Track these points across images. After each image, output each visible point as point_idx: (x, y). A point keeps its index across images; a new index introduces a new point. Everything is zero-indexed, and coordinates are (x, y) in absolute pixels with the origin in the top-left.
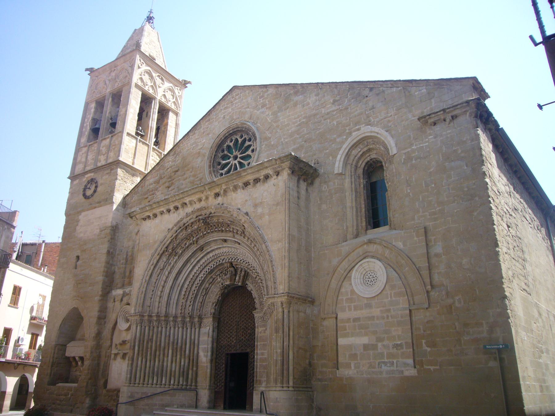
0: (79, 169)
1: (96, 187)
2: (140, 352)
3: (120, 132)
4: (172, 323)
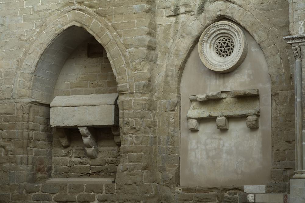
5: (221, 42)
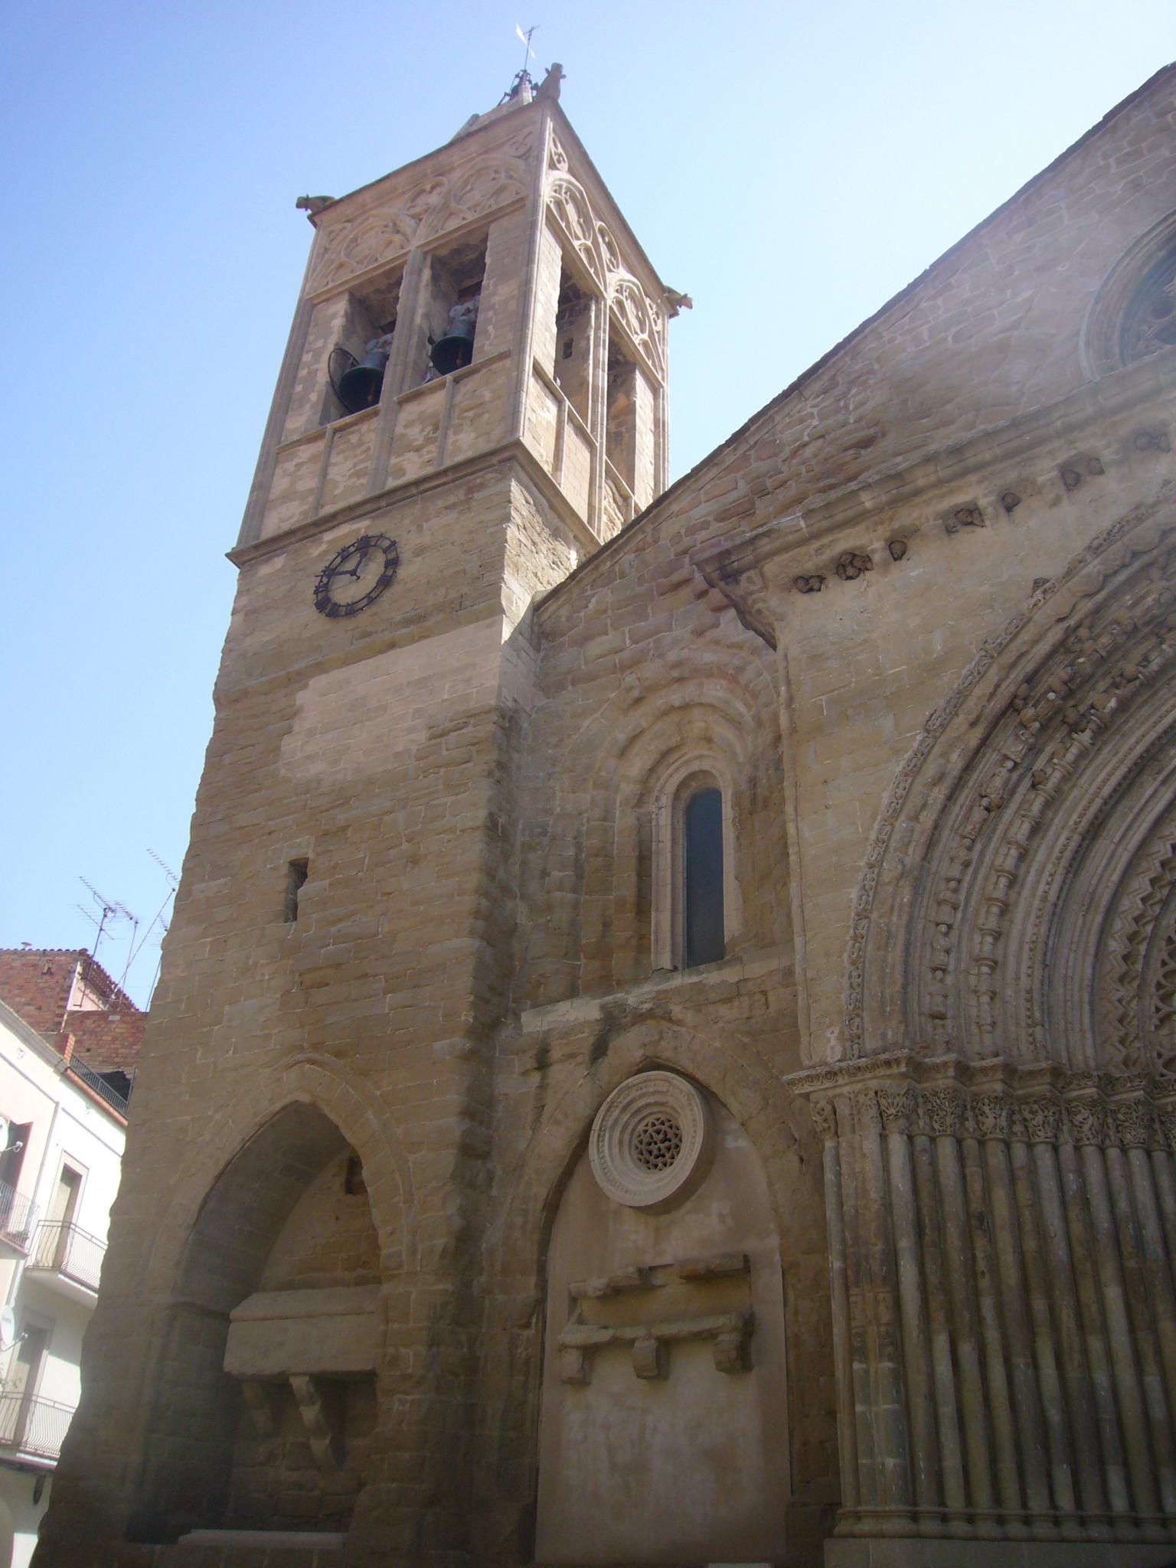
0: (281, 518)
1: (393, 564)
2: (935, 1303)
3: (502, 356)
4: (1087, 1120)
5: (651, 1130)
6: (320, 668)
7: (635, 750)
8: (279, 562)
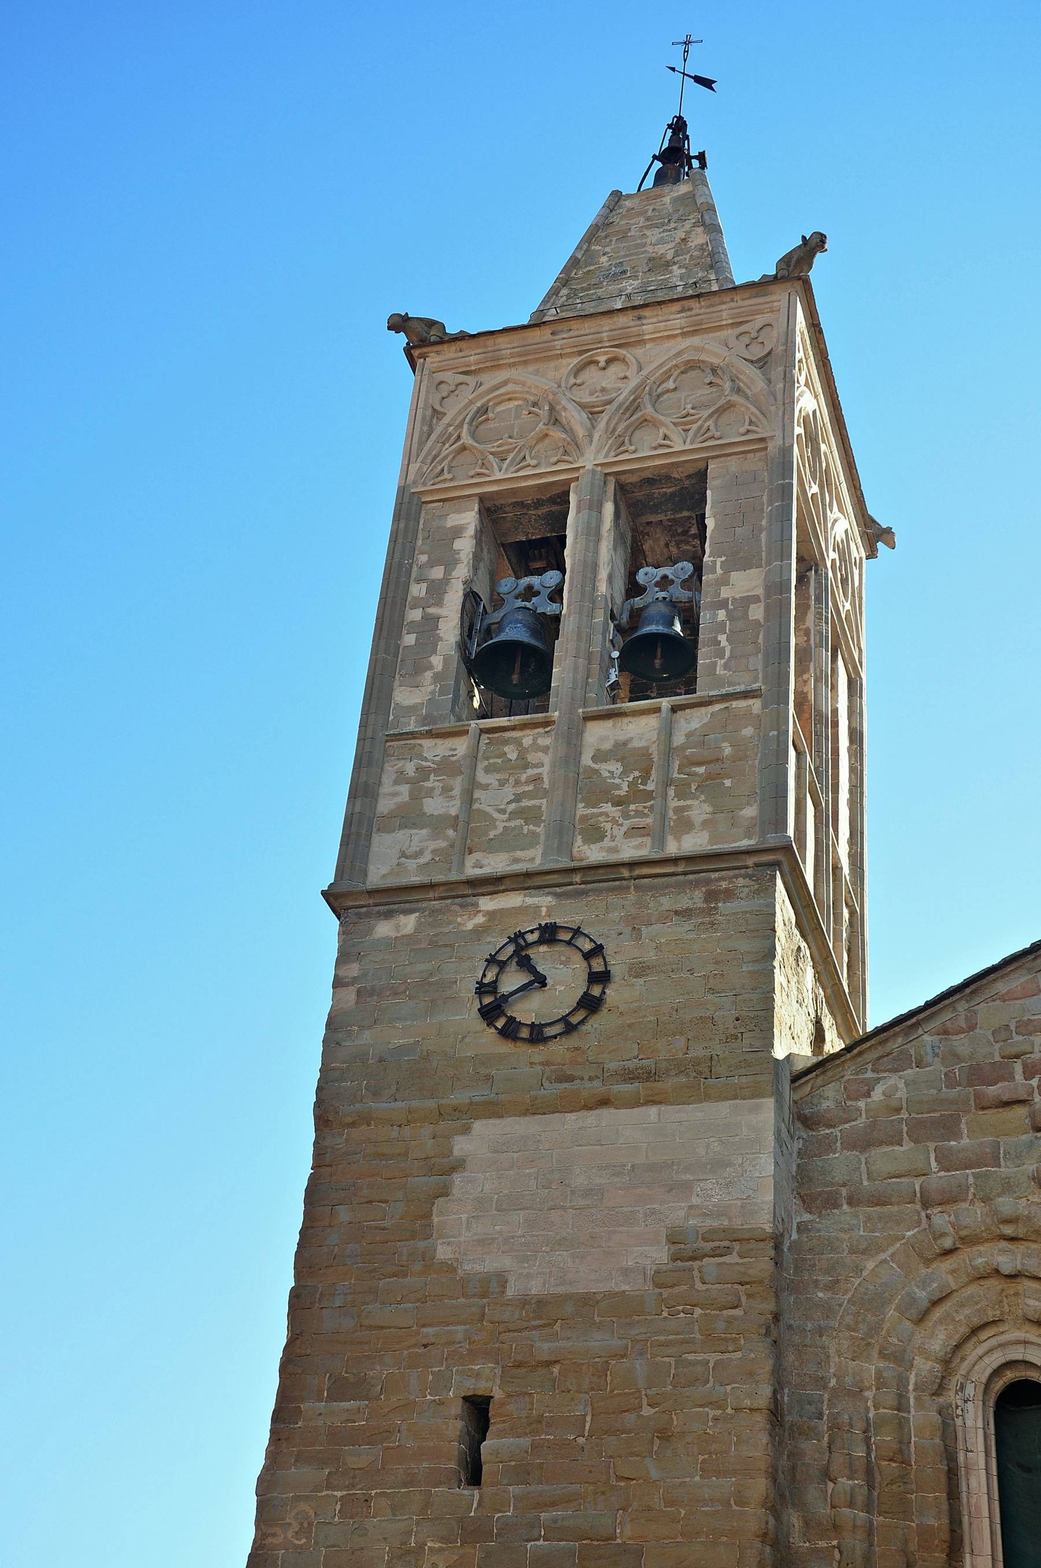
6: (493, 1110)
7: (938, 1313)
8: (408, 923)
